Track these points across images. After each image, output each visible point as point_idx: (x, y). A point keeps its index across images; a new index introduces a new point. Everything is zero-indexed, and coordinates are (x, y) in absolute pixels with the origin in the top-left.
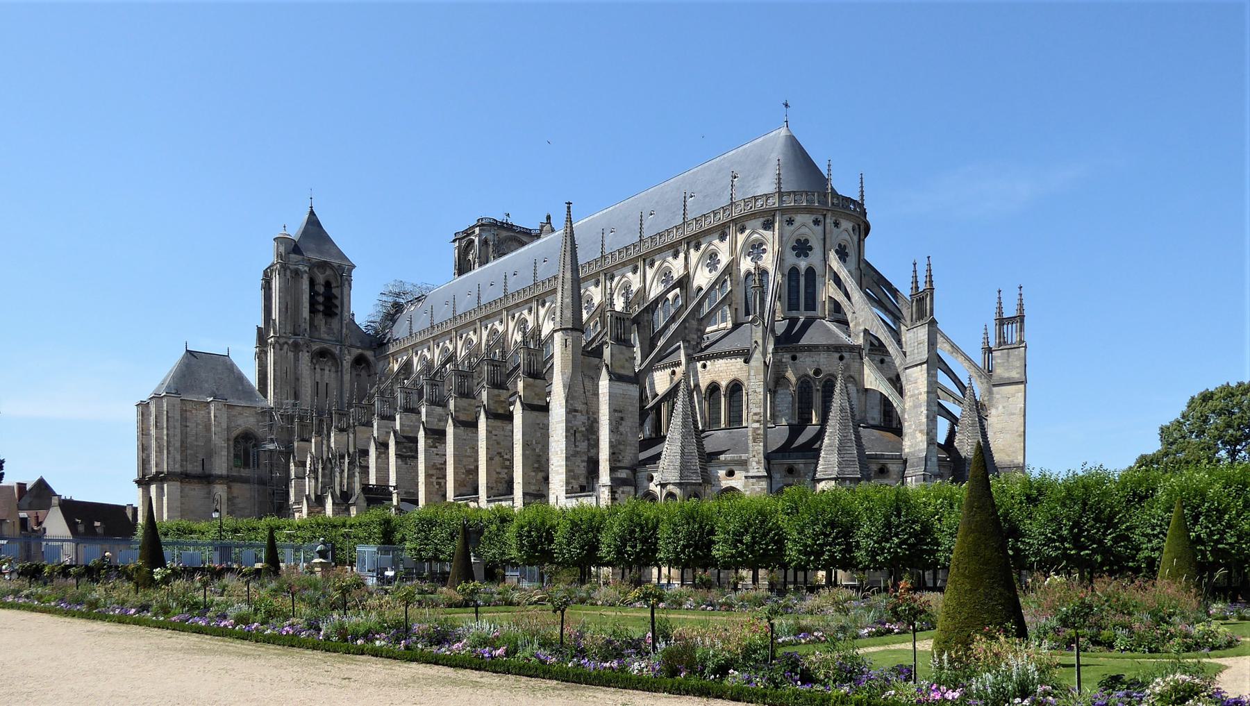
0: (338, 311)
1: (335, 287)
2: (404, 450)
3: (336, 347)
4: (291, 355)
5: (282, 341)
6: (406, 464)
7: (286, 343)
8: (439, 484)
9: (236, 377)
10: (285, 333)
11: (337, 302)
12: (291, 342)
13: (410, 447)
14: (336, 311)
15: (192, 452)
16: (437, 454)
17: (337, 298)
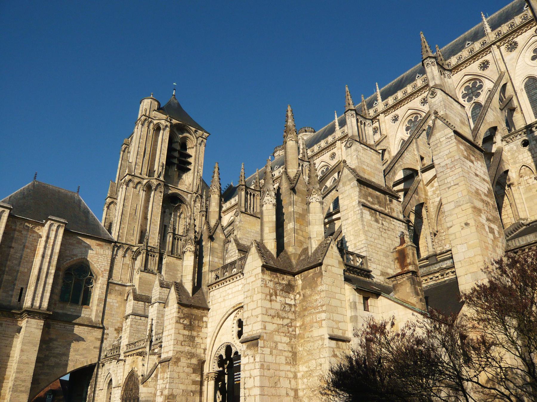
0: (191, 167)
1: (190, 148)
2: (370, 199)
3: (187, 195)
4: (142, 194)
5: (136, 180)
6: (377, 221)
7: (139, 183)
8: (492, 231)
9: (82, 209)
10: (141, 174)
11: (191, 160)
12: (145, 182)
13: (377, 197)
14: (189, 167)
15: (10, 278)
16: (477, 175)
17: (190, 156)
